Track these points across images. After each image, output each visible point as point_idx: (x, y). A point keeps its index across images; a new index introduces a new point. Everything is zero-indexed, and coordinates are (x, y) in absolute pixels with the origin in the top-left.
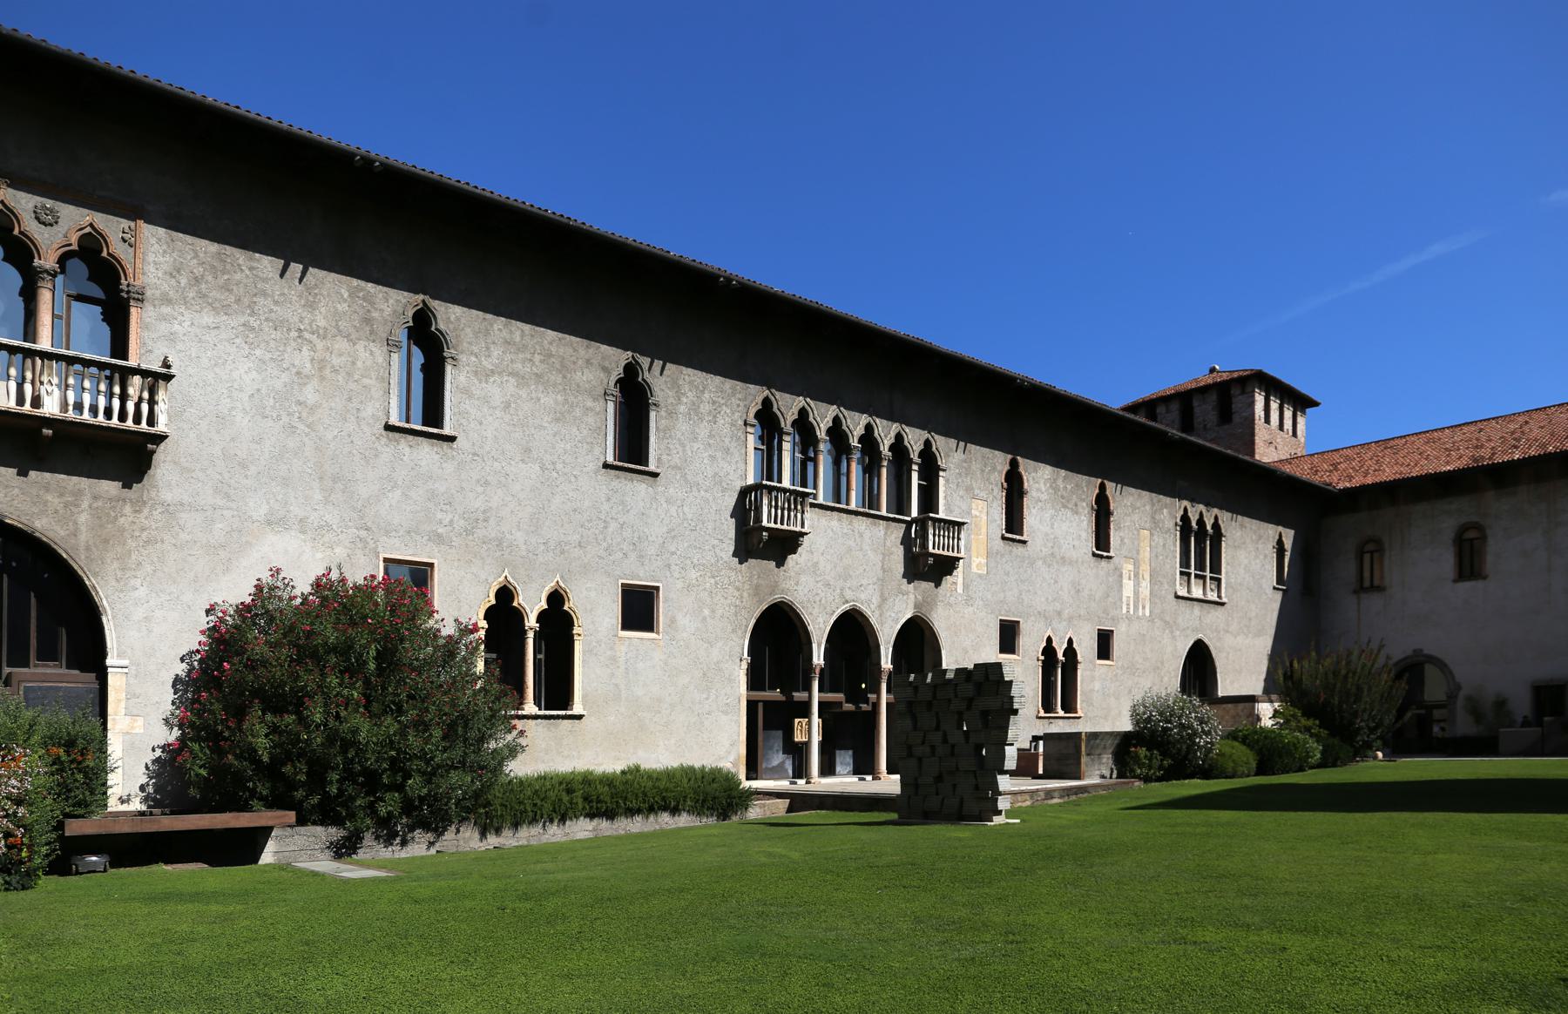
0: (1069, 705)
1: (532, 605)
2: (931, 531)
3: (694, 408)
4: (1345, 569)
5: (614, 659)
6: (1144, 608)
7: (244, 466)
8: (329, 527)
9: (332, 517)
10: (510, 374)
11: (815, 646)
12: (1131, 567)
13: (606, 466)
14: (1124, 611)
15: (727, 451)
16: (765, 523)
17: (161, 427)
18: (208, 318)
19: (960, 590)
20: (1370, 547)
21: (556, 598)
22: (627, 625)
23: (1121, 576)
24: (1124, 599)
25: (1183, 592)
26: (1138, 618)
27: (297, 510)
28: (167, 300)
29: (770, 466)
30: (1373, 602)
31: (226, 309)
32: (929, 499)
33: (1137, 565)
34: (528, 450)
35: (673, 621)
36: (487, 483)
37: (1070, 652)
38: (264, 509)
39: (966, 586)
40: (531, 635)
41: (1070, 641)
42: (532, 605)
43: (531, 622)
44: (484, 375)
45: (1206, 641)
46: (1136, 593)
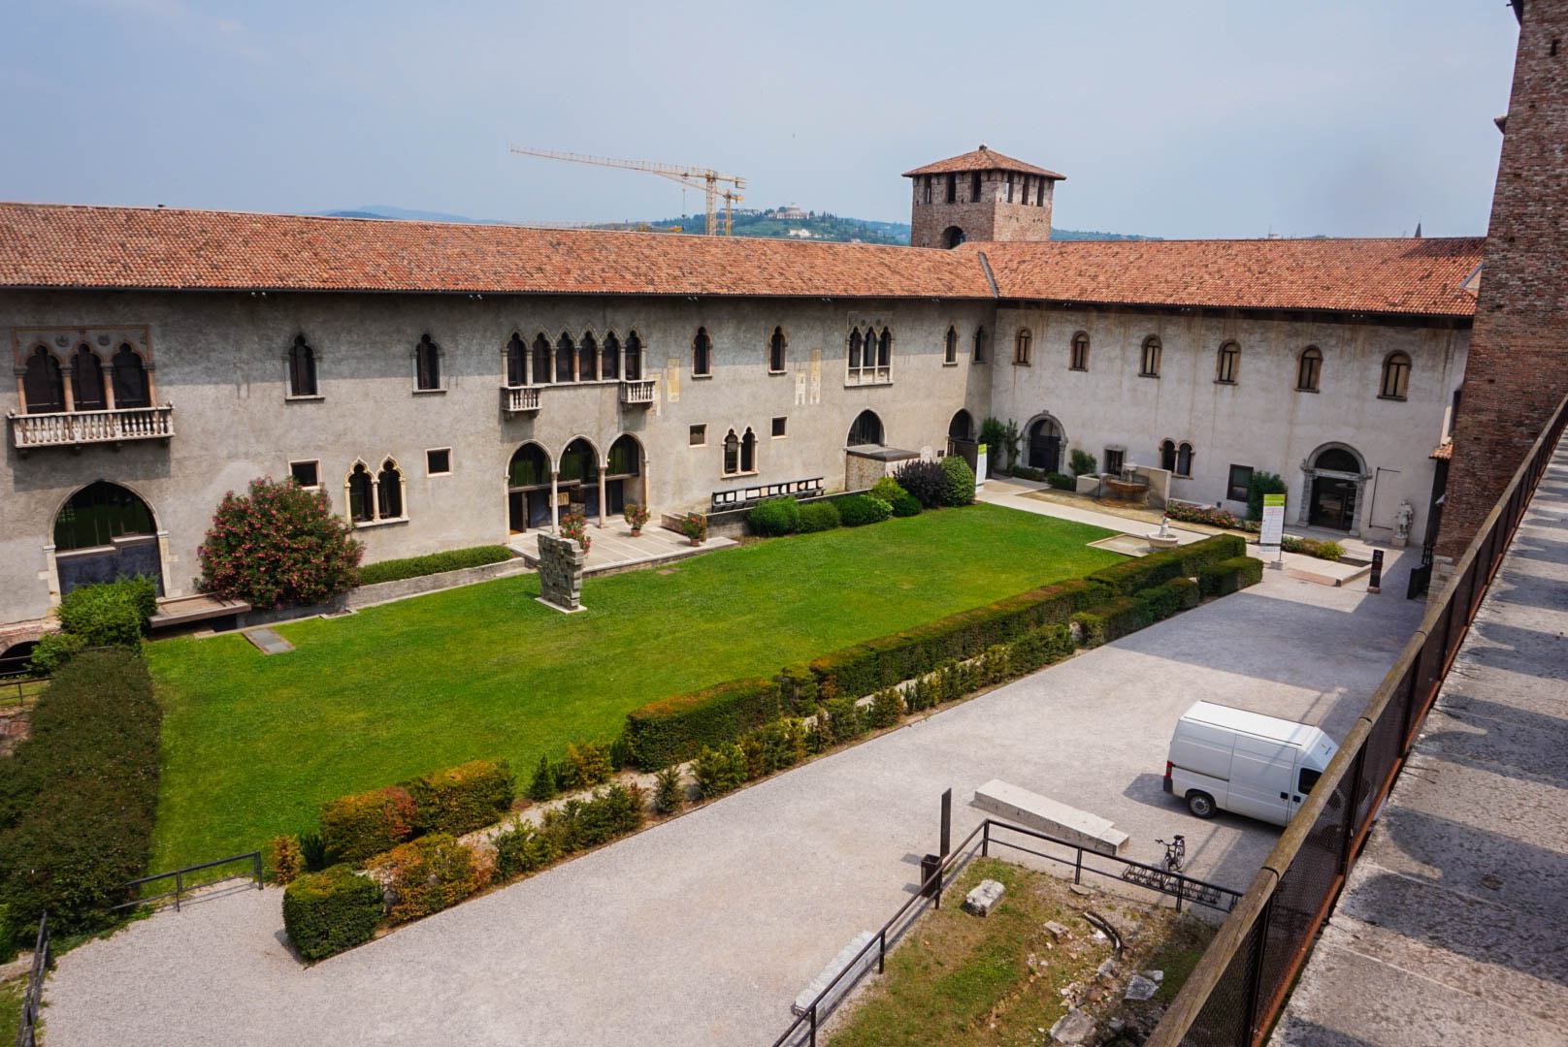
0: (747, 465)
1: (375, 472)
2: (630, 393)
3: (467, 350)
4: (1007, 348)
5: (425, 490)
6: (814, 398)
7: (213, 434)
8: (261, 454)
9: (261, 449)
10: (353, 358)
11: (553, 463)
13: (415, 394)
14: (797, 403)
16: (512, 409)
17: (171, 432)
18: (187, 370)
19: (658, 414)
20: (1025, 334)
21: (389, 465)
22: (432, 470)
23: (794, 382)
24: (797, 397)
25: (853, 382)
26: (810, 405)
28: (165, 366)
29: (517, 375)
30: (1023, 371)
31: (195, 362)
32: (634, 372)
34: (367, 395)
35: (459, 465)
36: (344, 416)
37: (749, 437)
38: (225, 453)
39: (663, 411)
41: (749, 429)
42: (375, 472)
43: (375, 479)
44: (340, 361)
45: (873, 410)
46: (808, 392)
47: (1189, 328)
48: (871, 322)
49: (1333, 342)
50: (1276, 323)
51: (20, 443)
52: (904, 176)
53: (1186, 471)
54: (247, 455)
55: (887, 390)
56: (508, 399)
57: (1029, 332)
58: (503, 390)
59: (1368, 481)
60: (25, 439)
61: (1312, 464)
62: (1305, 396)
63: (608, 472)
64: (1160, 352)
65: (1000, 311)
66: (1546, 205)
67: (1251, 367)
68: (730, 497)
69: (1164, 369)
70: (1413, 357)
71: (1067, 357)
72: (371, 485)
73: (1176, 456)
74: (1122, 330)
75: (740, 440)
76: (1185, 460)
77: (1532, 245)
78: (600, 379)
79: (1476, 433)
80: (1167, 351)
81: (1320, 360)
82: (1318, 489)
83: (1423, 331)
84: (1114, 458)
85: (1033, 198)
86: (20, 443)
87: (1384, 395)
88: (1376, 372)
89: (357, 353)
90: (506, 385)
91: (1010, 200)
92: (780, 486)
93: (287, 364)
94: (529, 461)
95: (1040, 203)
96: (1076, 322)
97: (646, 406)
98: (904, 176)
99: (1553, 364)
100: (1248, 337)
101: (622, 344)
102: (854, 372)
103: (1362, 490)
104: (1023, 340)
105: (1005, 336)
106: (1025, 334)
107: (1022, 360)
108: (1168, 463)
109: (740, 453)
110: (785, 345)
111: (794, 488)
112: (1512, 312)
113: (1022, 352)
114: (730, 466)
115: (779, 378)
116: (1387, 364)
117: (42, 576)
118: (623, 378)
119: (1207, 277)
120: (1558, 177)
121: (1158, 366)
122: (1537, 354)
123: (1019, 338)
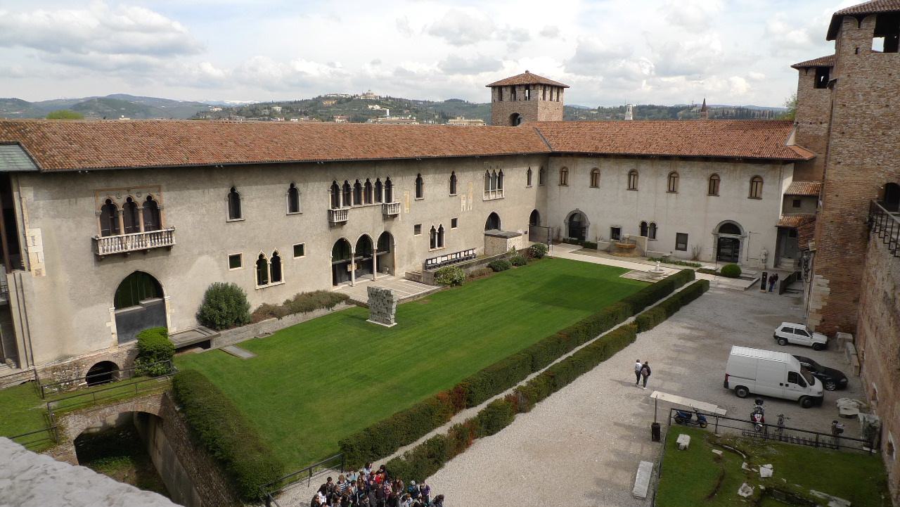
1: (268, 258)
4: (555, 177)
12: (465, 196)
15: (323, 200)
16: (335, 221)
17: (174, 243)
18: (179, 208)
20: (564, 170)
27: (206, 250)
28: (169, 206)
29: (335, 203)
30: (564, 189)
31: (183, 204)
32: (389, 199)
33: (467, 195)
35: (309, 252)
37: (441, 229)
40: (269, 266)
42: (268, 258)
43: (269, 262)
44: (251, 200)
47: (652, 166)
48: (494, 169)
49: (725, 171)
50: (696, 162)
51: (101, 253)
52: (487, 86)
53: (654, 236)
54: (207, 252)
55: (501, 201)
56: (333, 216)
57: (567, 169)
58: (329, 211)
59: (745, 239)
60: (104, 251)
61: (718, 230)
62: (712, 197)
63: (377, 251)
64: (638, 178)
65: (551, 158)
66: (856, 118)
67: (684, 184)
68: (434, 261)
69: (640, 186)
70: (764, 179)
71: (588, 181)
72: (266, 265)
73: (648, 229)
74: (617, 167)
75: (437, 231)
76: (652, 231)
77: (852, 136)
78: (374, 204)
79: (831, 219)
80: (641, 176)
81: (719, 180)
82: (721, 244)
83: (768, 166)
84: (616, 232)
85: (555, 97)
86: (101, 253)
87: (751, 197)
88: (747, 185)
89: (260, 195)
90: (330, 208)
91: (544, 99)
92: (456, 254)
93: (228, 202)
94: (341, 248)
95: (558, 100)
96: (592, 163)
97: (395, 216)
98: (487, 86)
99: (863, 188)
100: (683, 169)
101: (383, 184)
102: (487, 192)
103: (742, 243)
104: (564, 173)
105: (554, 171)
106: (564, 170)
107: (563, 183)
108: (644, 232)
109: (437, 238)
110: (456, 181)
111: (462, 255)
112: (845, 165)
113: (563, 179)
114: (433, 245)
115: (454, 198)
116: (752, 181)
117: (108, 325)
118: (384, 201)
119: (659, 140)
120: (861, 106)
121: (637, 185)
122: (856, 183)
123: (561, 172)
